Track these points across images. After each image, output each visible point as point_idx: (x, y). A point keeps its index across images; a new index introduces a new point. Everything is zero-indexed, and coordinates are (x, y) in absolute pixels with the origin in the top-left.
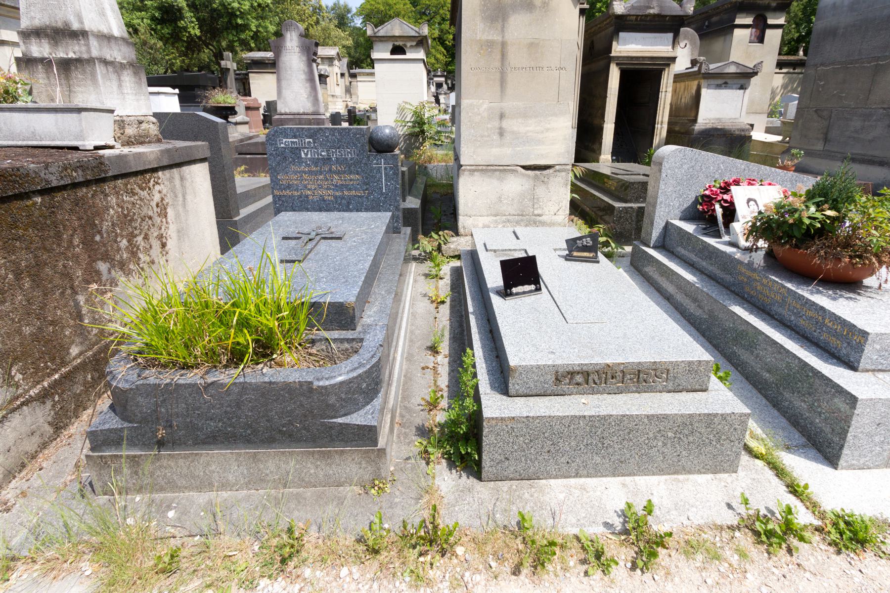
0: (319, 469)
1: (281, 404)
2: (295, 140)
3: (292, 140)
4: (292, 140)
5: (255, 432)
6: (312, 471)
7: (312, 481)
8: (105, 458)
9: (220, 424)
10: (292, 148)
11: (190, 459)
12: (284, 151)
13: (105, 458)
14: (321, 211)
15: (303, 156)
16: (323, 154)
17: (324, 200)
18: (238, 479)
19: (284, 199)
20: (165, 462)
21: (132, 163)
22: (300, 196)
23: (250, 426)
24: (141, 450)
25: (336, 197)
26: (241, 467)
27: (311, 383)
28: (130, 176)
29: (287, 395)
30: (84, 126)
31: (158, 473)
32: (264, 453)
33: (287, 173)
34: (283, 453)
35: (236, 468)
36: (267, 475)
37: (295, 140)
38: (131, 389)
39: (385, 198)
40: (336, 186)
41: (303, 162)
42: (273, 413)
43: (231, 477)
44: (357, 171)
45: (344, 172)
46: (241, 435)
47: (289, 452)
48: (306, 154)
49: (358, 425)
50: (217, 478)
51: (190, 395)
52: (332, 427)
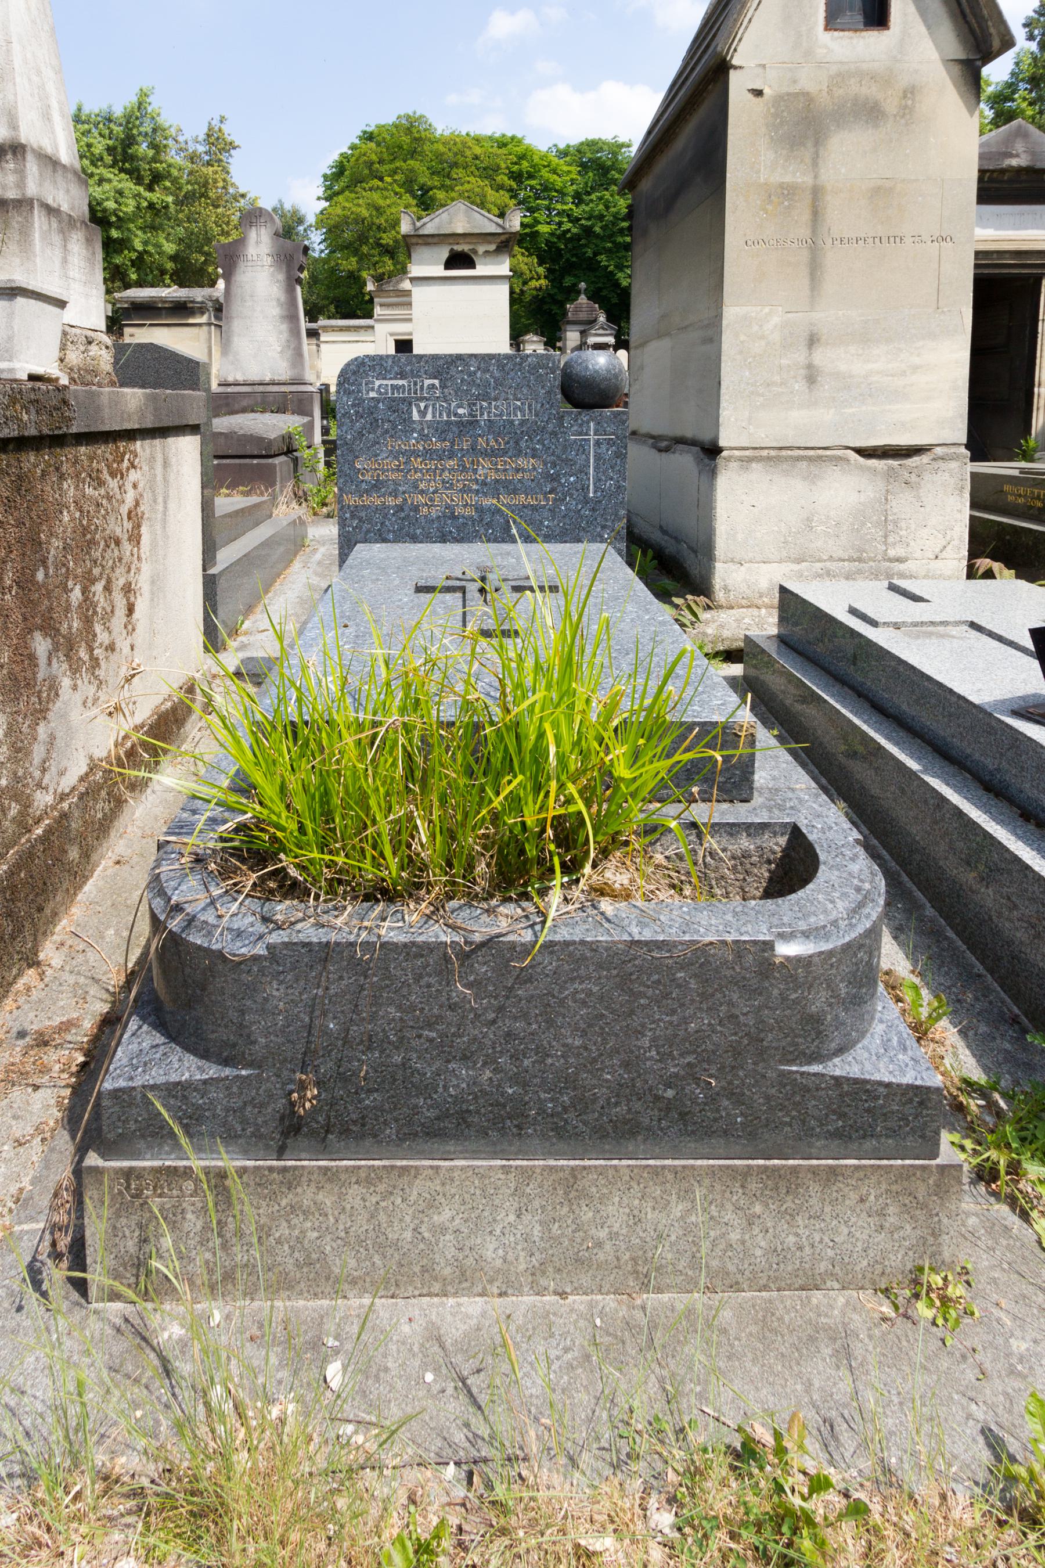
0: (756, 1230)
1: (673, 1012)
2: (400, 382)
3: (395, 382)
4: (395, 382)
5: (582, 1104)
6: (734, 1236)
7: (732, 1268)
8: (139, 1177)
9: (488, 1074)
10: (394, 400)
11: (381, 1187)
12: (376, 407)
13: (139, 1177)
14: (444, 542)
15: (416, 416)
16: (460, 411)
17: (453, 517)
18: (510, 1257)
19: (363, 514)
20: (306, 1195)
21: (106, 412)
22: (400, 508)
23: (571, 1082)
24: (246, 1154)
25: (479, 509)
26: (527, 1218)
27: (769, 946)
28: (97, 442)
29: (693, 985)
30: (16, 328)
31: (283, 1230)
32: (601, 1171)
33: (376, 455)
34: (656, 1171)
35: (512, 1218)
36: (599, 1245)
37: (400, 382)
38: (256, 958)
39: (593, 510)
40: (484, 483)
41: (413, 430)
42: (646, 1042)
43: (491, 1251)
44: (534, 450)
45: (505, 453)
46: (541, 1111)
47: (675, 1170)
48: (423, 413)
49: (888, 1085)
50: (451, 1252)
51: (418, 978)
52: (807, 1088)
